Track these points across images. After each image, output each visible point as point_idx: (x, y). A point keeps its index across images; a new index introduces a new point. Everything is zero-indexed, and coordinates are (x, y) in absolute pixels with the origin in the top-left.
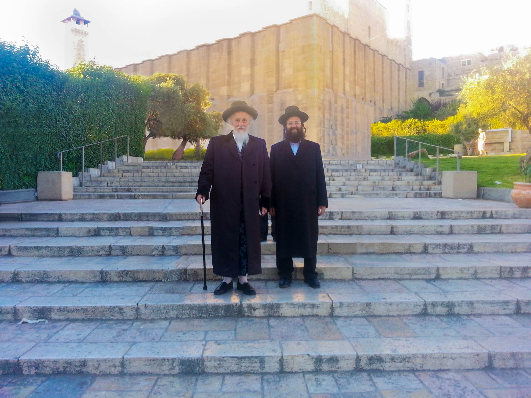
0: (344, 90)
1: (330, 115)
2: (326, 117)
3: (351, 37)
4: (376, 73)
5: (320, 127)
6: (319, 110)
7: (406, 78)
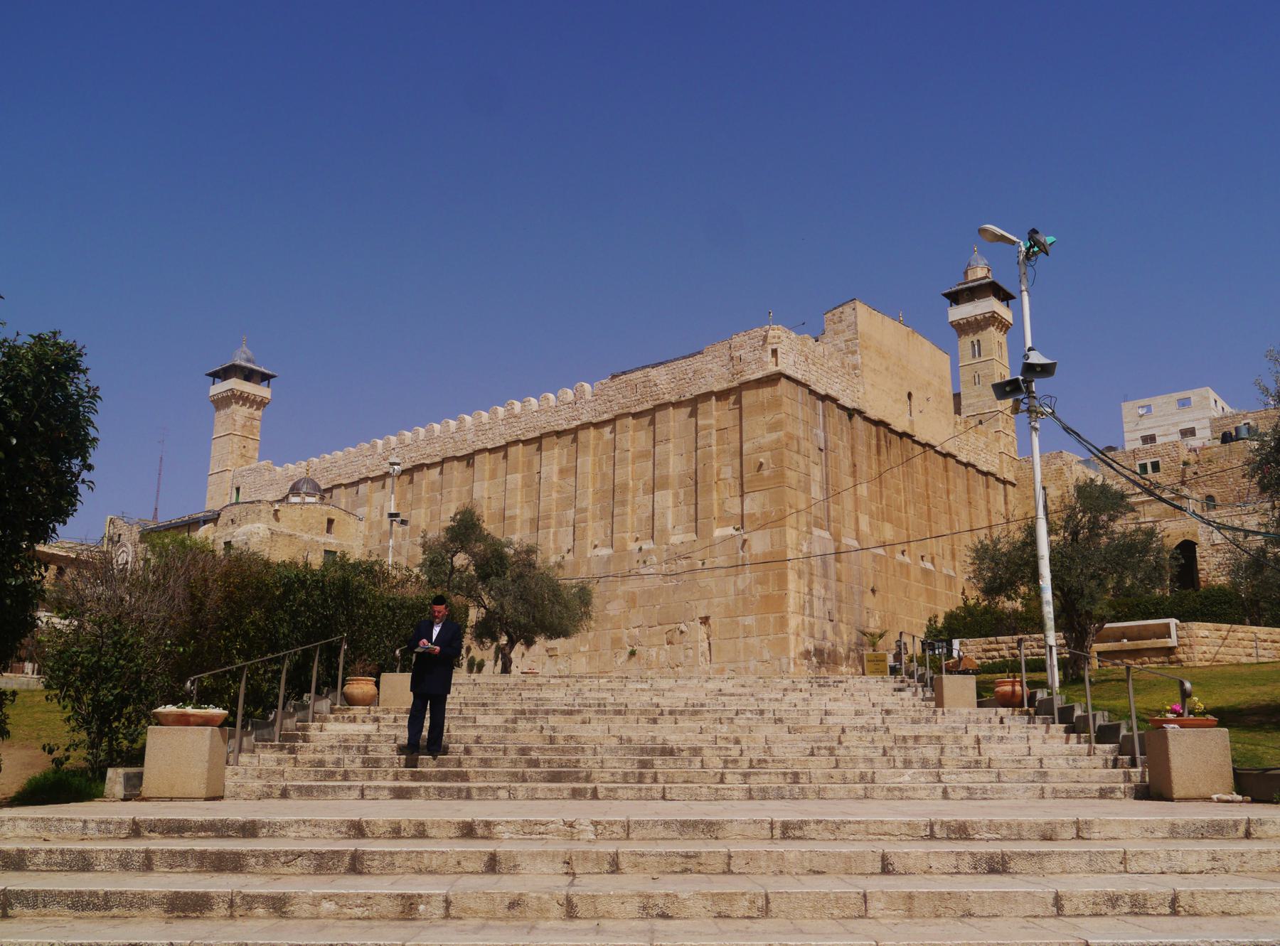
0: (857, 530)
1: (826, 588)
2: (815, 592)
3: (867, 419)
4: (930, 493)
5: (804, 615)
6: (800, 577)
7: (1006, 503)
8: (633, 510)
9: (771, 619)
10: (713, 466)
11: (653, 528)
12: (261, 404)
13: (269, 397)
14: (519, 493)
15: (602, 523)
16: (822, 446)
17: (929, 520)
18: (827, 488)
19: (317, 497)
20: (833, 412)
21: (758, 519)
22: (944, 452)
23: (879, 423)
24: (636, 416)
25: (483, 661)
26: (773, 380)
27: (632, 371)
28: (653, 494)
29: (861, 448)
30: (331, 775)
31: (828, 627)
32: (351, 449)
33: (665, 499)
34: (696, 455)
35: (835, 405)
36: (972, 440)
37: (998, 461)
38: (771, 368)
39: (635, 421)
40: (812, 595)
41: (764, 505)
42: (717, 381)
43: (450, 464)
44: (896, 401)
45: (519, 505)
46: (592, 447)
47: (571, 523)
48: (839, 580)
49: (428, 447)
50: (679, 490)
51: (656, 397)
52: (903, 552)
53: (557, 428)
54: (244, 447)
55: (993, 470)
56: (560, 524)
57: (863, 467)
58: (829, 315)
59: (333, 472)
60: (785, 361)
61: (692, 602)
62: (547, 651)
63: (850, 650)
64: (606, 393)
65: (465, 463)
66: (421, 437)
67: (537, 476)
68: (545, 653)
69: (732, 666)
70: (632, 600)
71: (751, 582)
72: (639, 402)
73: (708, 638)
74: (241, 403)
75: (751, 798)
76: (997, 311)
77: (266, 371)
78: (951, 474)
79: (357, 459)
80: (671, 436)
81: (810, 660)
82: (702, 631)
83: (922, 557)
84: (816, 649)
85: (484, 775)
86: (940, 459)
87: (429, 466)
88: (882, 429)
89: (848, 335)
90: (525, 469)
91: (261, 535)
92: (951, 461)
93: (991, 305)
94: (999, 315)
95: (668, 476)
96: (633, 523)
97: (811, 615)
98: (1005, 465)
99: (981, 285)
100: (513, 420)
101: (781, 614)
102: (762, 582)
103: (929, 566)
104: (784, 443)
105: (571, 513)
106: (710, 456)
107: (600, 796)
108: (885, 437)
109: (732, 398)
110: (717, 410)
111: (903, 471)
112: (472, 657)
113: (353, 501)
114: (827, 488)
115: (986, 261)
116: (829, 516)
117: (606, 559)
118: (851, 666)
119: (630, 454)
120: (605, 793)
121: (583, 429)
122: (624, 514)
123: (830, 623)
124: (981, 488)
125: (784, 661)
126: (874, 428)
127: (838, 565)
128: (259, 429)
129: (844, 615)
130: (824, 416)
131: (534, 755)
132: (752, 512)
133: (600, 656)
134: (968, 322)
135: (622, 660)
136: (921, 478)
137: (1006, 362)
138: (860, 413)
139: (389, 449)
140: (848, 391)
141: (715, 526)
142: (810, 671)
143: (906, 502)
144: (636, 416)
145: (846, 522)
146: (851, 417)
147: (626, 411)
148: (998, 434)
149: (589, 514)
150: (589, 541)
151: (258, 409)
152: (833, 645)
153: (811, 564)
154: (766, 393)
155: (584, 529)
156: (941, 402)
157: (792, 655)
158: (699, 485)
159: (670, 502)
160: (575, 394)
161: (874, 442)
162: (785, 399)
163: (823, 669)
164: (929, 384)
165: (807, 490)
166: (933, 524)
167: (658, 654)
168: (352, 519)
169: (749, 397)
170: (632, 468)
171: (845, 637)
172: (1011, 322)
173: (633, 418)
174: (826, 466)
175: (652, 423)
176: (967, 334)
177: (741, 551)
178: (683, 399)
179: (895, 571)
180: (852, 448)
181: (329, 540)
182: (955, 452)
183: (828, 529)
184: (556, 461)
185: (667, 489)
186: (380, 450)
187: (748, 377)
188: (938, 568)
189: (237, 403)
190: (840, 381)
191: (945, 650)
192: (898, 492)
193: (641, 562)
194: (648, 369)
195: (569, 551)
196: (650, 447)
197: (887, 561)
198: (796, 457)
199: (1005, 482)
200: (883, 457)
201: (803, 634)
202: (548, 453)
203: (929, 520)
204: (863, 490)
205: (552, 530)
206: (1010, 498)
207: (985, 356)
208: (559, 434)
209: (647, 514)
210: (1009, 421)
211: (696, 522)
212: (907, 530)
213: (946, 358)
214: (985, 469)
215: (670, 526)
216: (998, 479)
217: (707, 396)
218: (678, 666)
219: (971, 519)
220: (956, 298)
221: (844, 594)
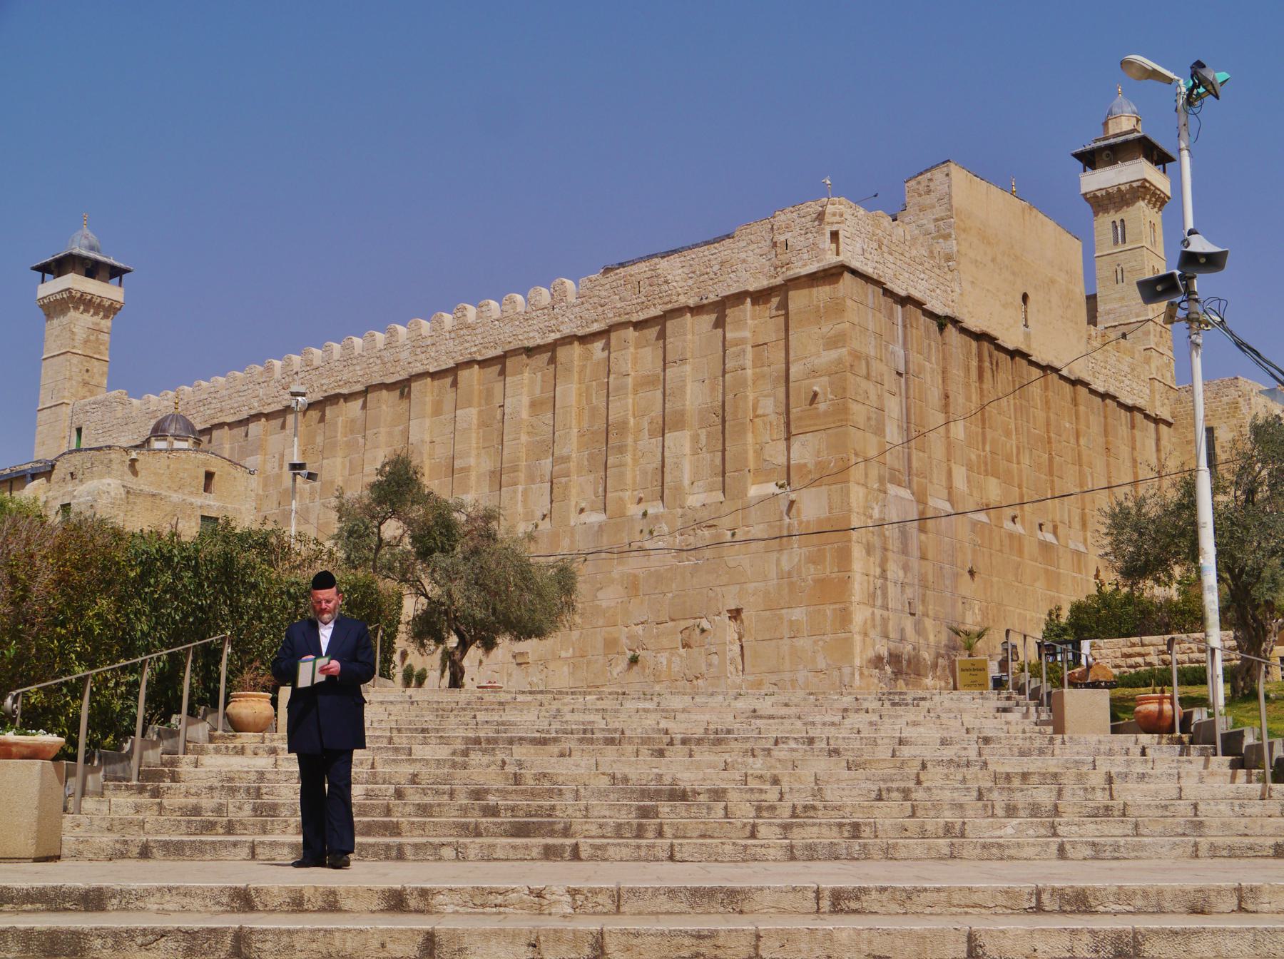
0: (950, 488)
1: (906, 568)
2: (890, 575)
3: (965, 331)
4: (1052, 435)
5: (874, 606)
6: (869, 553)
7: (1158, 450)
8: (634, 460)
9: (829, 612)
10: (746, 397)
11: (663, 485)
12: (110, 310)
13: (122, 301)
14: (474, 435)
15: (591, 477)
16: (902, 370)
17: (1051, 473)
18: (908, 427)
19: (191, 441)
20: (917, 319)
21: (810, 472)
22: (1073, 378)
23: (981, 337)
24: (639, 325)
25: (424, 670)
26: (832, 275)
27: (634, 262)
28: (663, 435)
29: (956, 373)
30: (209, 827)
31: (909, 623)
32: (237, 373)
33: (679, 442)
34: (724, 381)
35: (919, 312)
36: (1112, 360)
37: (1148, 391)
38: (830, 259)
39: (637, 334)
40: (886, 579)
41: (819, 452)
42: (753, 276)
43: (376, 394)
44: (1005, 306)
45: (474, 453)
46: (576, 369)
47: (548, 478)
48: (923, 558)
49: (346, 370)
51: (667, 299)
52: (1014, 519)
53: (527, 344)
54: (87, 371)
55: (1140, 403)
56: (531, 479)
57: (959, 400)
58: (913, 183)
59: (213, 406)
60: (850, 248)
61: (718, 589)
62: (514, 657)
63: (938, 655)
64: (596, 293)
65: (398, 392)
66: (336, 355)
67: (499, 411)
68: (511, 660)
69: (774, 678)
70: (633, 586)
71: (800, 561)
73: (740, 639)
74: (82, 308)
75: (793, 858)
76: (1148, 178)
77: (117, 263)
78: (1082, 408)
79: (245, 388)
80: (689, 355)
81: (882, 669)
82: (732, 629)
83: (1041, 525)
84: (890, 655)
85: (423, 826)
86: (1067, 387)
87: (348, 397)
88: (986, 345)
89: (939, 212)
91: (112, 494)
92: (1082, 391)
93: (1140, 169)
94: (1151, 184)
95: (683, 410)
97: (885, 607)
98: (1157, 397)
99: (1126, 142)
100: (465, 331)
101: (842, 606)
102: (815, 560)
103: (1050, 538)
104: (848, 364)
105: (547, 463)
106: (743, 383)
107: (583, 855)
108: (991, 356)
109: (775, 301)
110: (753, 318)
111: (1015, 404)
112: (410, 665)
114: (908, 429)
115: (1134, 108)
116: (910, 468)
117: (596, 528)
118: (940, 679)
119: (630, 380)
120: (590, 851)
122: (622, 465)
123: (911, 617)
124: (1124, 428)
125: (847, 670)
126: (974, 344)
127: (923, 537)
129: (931, 607)
130: (905, 326)
131: (492, 800)
132: (802, 461)
133: (589, 663)
134: (1108, 194)
135: (619, 669)
136: (1040, 414)
137: (1160, 250)
138: (955, 322)
139: (289, 373)
140: (938, 291)
141: (750, 480)
142: (882, 684)
143: (1018, 448)
144: (639, 325)
145: (935, 476)
146: (942, 328)
147: (624, 318)
148: (1148, 352)
149: (573, 465)
150: (573, 503)
151: (106, 317)
152: (914, 649)
153: (884, 536)
154: (822, 293)
155: (566, 487)
156: (1068, 307)
157: (857, 662)
158: (727, 423)
159: (687, 449)
160: (552, 295)
161: (974, 363)
162: (849, 303)
163: (901, 682)
164: (1053, 282)
165: (879, 431)
166: (1056, 478)
167: (669, 661)
168: (239, 473)
169: (798, 299)
170: (634, 399)
171: (931, 637)
172: (1169, 194)
173: (635, 329)
174: (907, 398)
175: (662, 335)
176: (1106, 211)
177: (786, 517)
178: (705, 302)
179: (1002, 545)
180: (943, 372)
181: (207, 502)
182: (1088, 378)
183: (910, 487)
184: (525, 389)
186: (278, 373)
187: (797, 270)
188: (1062, 540)
189: (76, 308)
190: (926, 277)
191: (1070, 656)
192: (1008, 434)
193: (646, 531)
194: (656, 260)
195: (545, 516)
196: (659, 370)
197: (991, 531)
198: (864, 384)
199: (1157, 421)
200: (987, 384)
201: (872, 634)
202: (515, 378)
203: (1051, 473)
204: (958, 430)
205: (520, 488)
206: (1164, 442)
207: (1132, 242)
208: (530, 351)
209: (655, 465)
210: (1164, 334)
211: (723, 476)
212: (1020, 487)
213: (1078, 245)
214: (1129, 402)
215: (686, 482)
216: (1147, 417)
217: (739, 298)
218: (697, 678)
219: (1109, 472)
220: (1090, 159)
221: (930, 578)
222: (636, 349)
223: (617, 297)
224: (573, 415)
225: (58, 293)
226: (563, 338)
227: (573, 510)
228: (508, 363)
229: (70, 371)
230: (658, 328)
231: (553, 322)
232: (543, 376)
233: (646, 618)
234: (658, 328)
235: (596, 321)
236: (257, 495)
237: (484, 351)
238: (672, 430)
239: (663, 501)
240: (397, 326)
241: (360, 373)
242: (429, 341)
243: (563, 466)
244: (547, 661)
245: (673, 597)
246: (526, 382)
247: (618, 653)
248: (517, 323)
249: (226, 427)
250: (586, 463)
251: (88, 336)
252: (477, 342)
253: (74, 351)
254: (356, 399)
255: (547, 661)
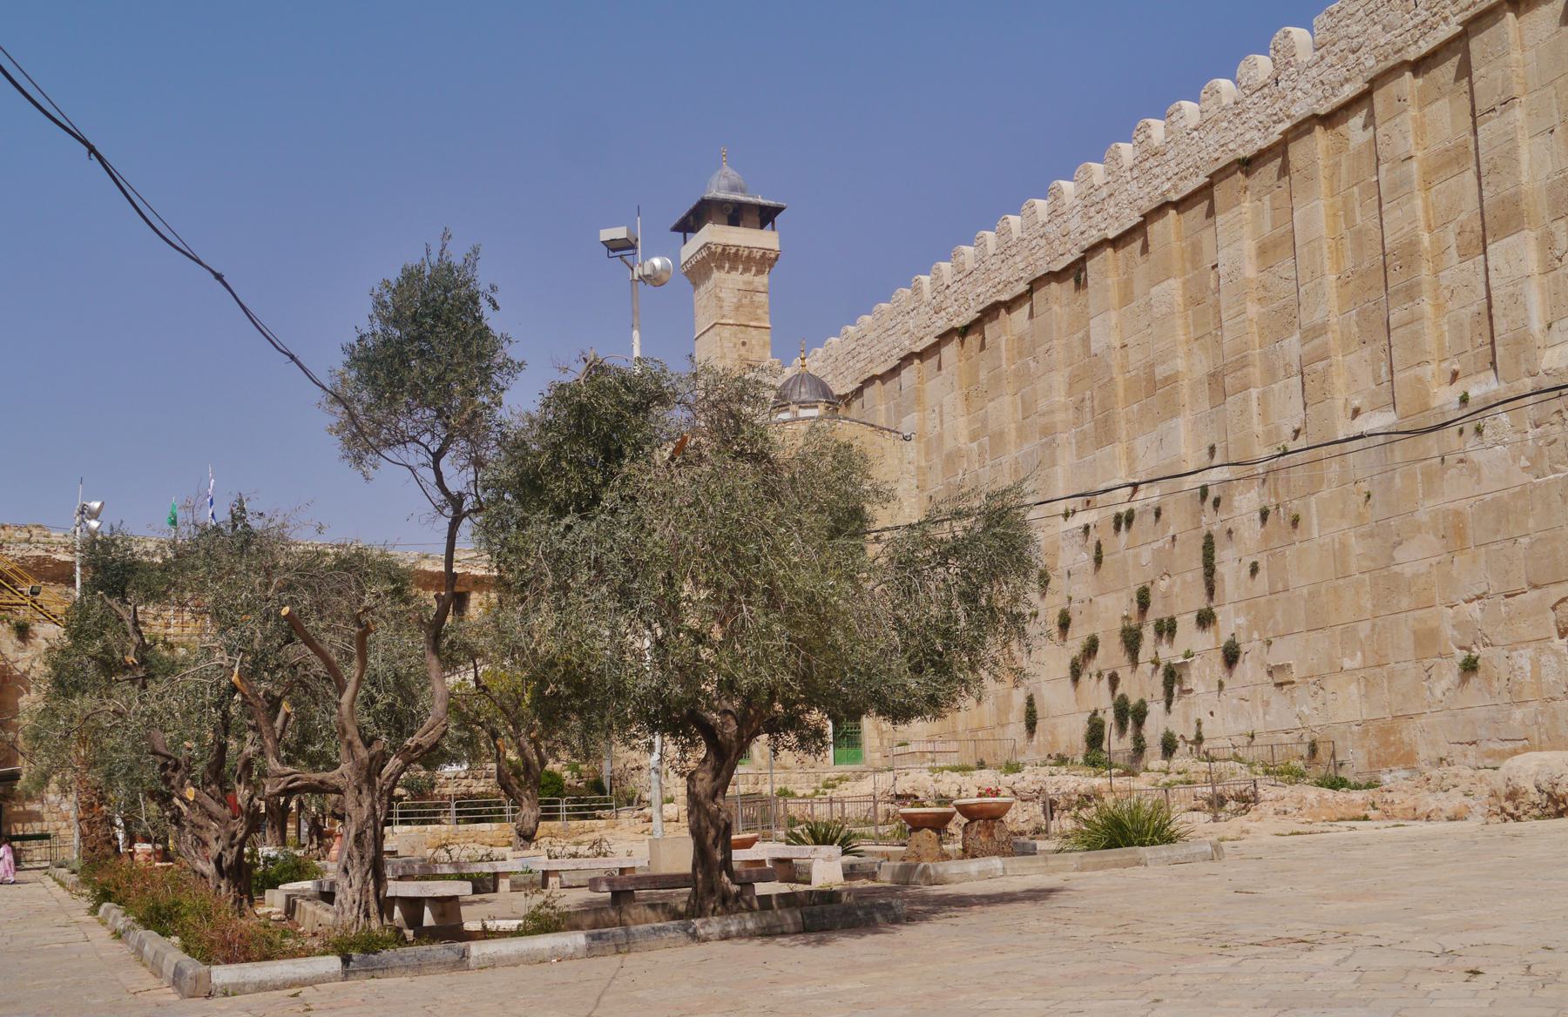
8: (1438, 307)
11: (1492, 342)
12: (764, 262)
14: (1179, 322)
15: (1366, 352)
24: (1419, 66)
25: (1142, 702)
28: (1485, 252)
32: (884, 305)
39: (1420, 81)
43: (1043, 291)
45: (1181, 350)
46: (1322, 173)
47: (1295, 368)
49: (1005, 267)
50: (1553, 227)
56: (1271, 374)
59: (862, 356)
62: (1270, 673)
64: (1342, 32)
65: (1072, 282)
66: (991, 249)
67: (1212, 275)
68: (1266, 678)
70: (1455, 533)
72: (1427, 27)
74: (727, 266)
77: (761, 200)
79: (894, 322)
87: (1010, 306)
90: (1188, 265)
96: (1441, 335)
105: (1293, 346)
112: (1122, 696)
113: (898, 405)
121: (1298, 137)
128: (766, 309)
133: (1391, 677)
135: (1444, 684)
139: (941, 289)
144: (1419, 66)
149: (1332, 339)
151: (759, 272)
155: (1325, 377)
159: (1532, 263)
160: (1274, 60)
167: (1536, 664)
170: (1425, 200)
173: (1416, 75)
175: (1465, 70)
185: (1519, 229)
186: (927, 294)
189: (720, 267)
195: (1297, 432)
202: (1229, 215)
208: (1247, 165)
209: (1475, 308)
215: (1536, 326)
222: (1421, 109)
223: (1379, 27)
224: (1325, 250)
225: (697, 252)
226: (1296, 127)
227: (1341, 414)
228: (1216, 193)
229: (722, 347)
230: (1456, 60)
231: (1280, 104)
232: (1273, 200)
233: (1484, 588)
234: (1456, 60)
235: (1347, 80)
236: (919, 468)
237: (1181, 185)
238: (1497, 237)
239: (1495, 369)
240: (1061, 182)
241: (1021, 266)
242: (1105, 192)
243: (1317, 342)
244: (1322, 677)
245: (1532, 545)
246: (1248, 216)
247: (1440, 655)
248: (1225, 124)
249: (878, 382)
250: (1355, 329)
251: (740, 300)
252: (1170, 174)
253: (723, 321)
254: (1021, 306)
255: (1322, 677)
